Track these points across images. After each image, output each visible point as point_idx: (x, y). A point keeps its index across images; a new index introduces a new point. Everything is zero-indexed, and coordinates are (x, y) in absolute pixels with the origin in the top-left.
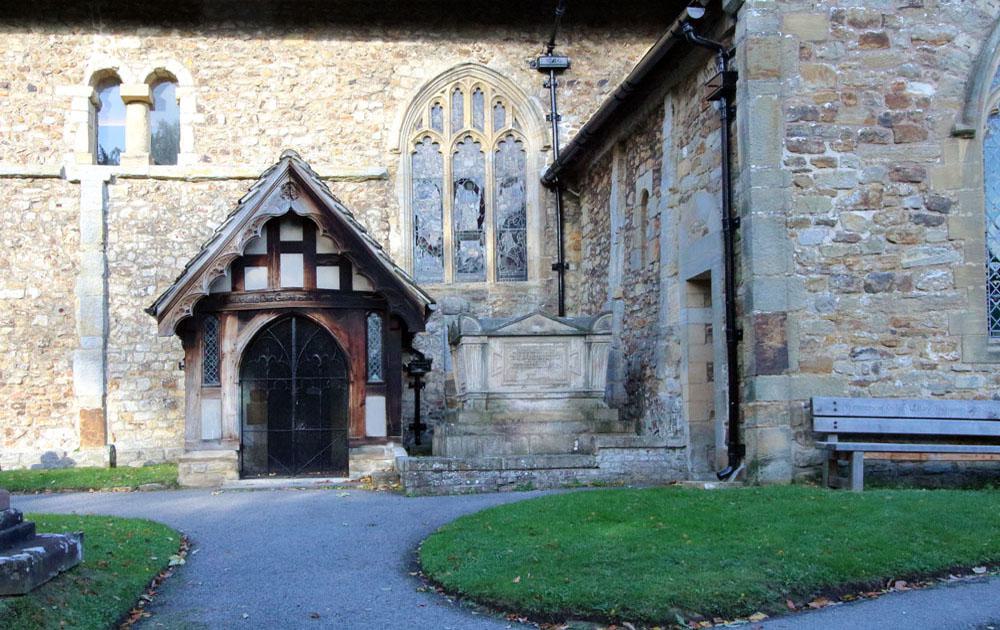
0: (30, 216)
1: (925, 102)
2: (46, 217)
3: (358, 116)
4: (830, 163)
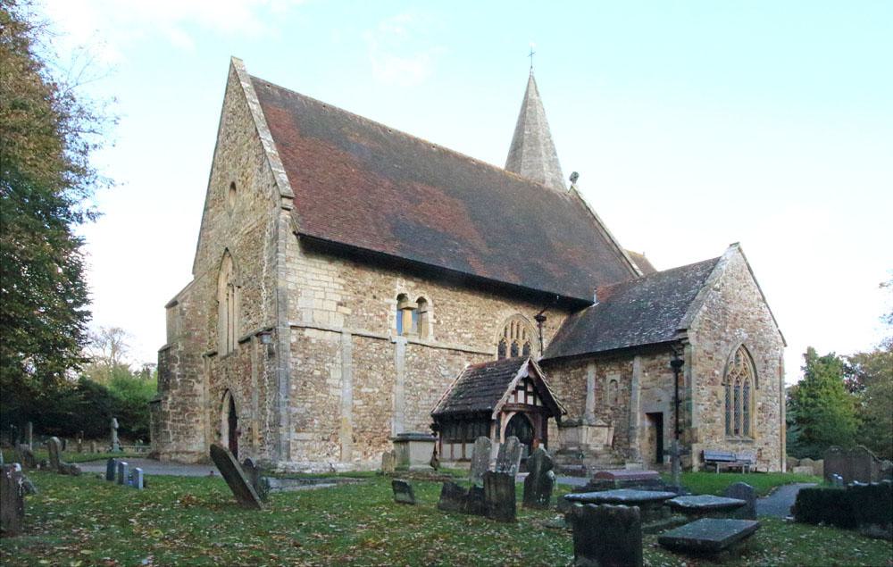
0: (376, 355)
2: (382, 357)
3: (486, 329)
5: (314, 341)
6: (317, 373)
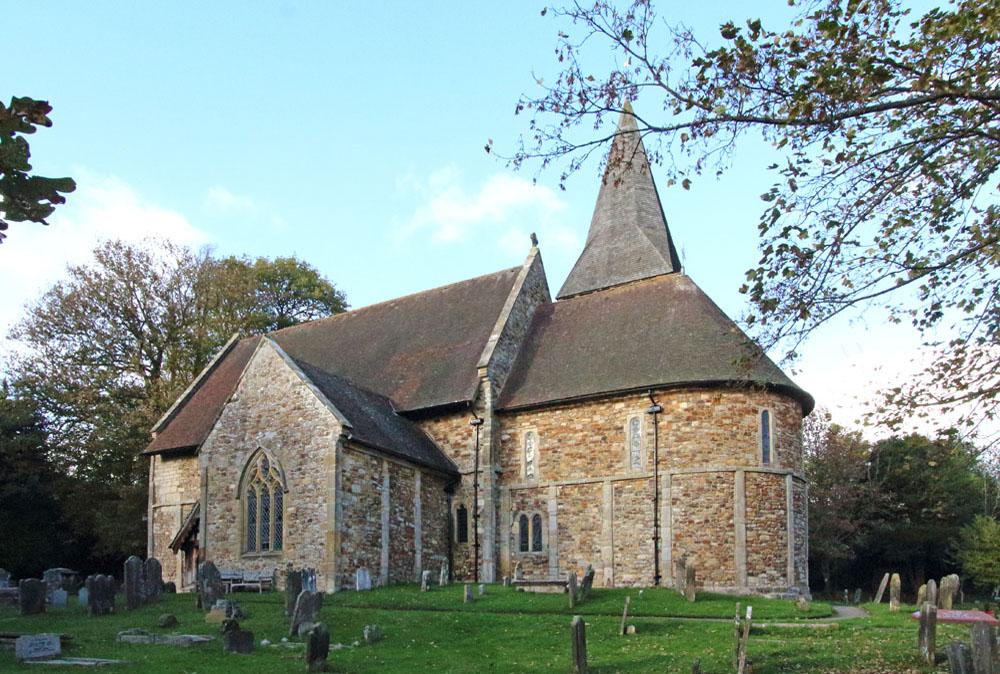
4: (215, 508)
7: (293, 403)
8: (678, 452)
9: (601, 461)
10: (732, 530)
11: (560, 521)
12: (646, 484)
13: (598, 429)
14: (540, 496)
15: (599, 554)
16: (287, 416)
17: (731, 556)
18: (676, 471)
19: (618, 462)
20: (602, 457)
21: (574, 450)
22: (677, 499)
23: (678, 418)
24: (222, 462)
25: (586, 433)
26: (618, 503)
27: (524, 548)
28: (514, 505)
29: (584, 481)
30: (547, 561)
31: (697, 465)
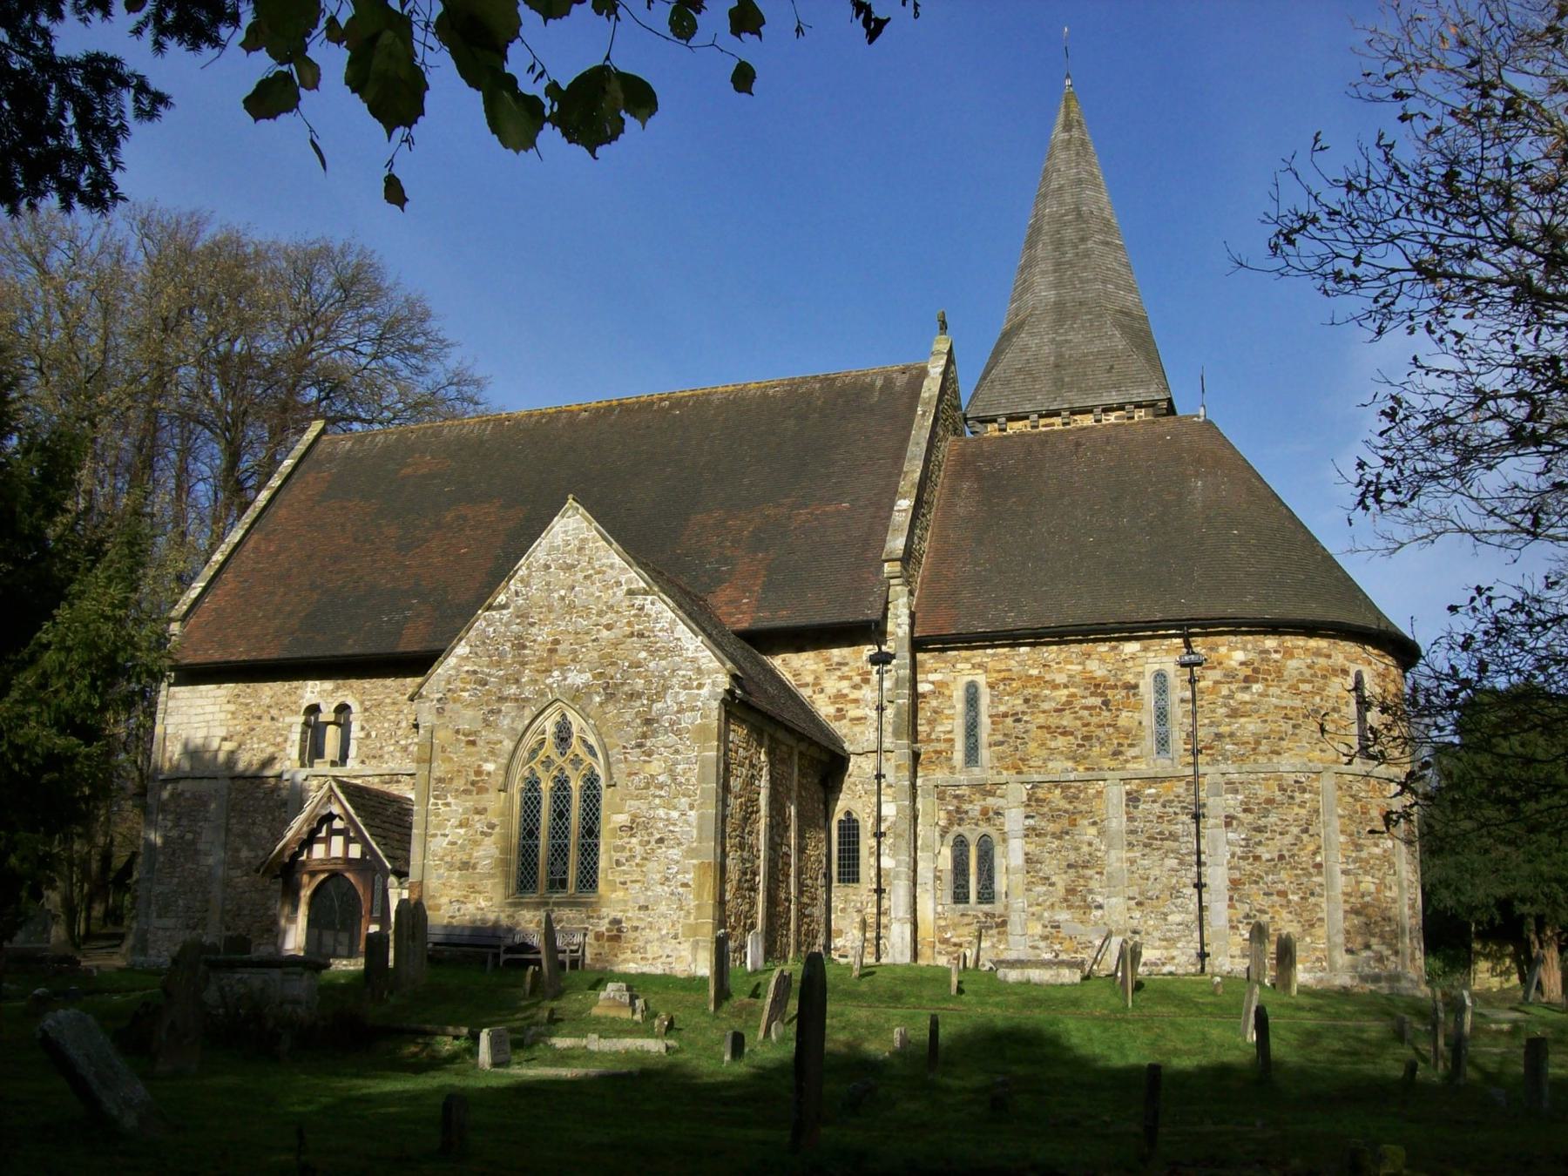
1: (489, 774)
4: (448, 805)
5: (188, 795)
6: (189, 836)
7: (629, 624)
8: (1232, 735)
9: (1102, 744)
10: (1320, 874)
11: (1031, 848)
12: (1180, 788)
13: (1096, 687)
14: (990, 801)
15: (1099, 913)
16: (616, 645)
17: (1321, 920)
18: (1230, 767)
19: (1131, 745)
20: (1102, 735)
21: (1054, 721)
22: (1233, 818)
23: (1230, 676)
24: (468, 718)
25: (1072, 690)
26: (1131, 819)
27: (960, 896)
28: (943, 814)
29: (1072, 777)
30: (1004, 923)
31: (1262, 759)
